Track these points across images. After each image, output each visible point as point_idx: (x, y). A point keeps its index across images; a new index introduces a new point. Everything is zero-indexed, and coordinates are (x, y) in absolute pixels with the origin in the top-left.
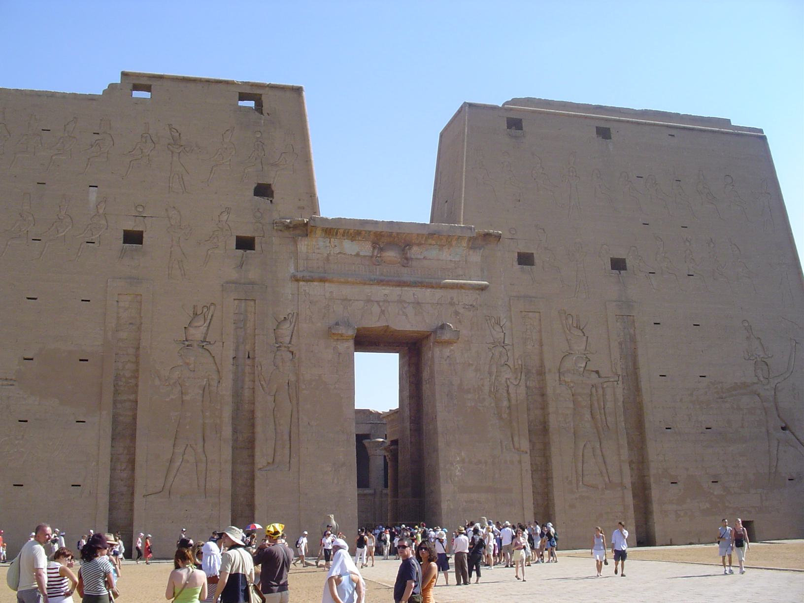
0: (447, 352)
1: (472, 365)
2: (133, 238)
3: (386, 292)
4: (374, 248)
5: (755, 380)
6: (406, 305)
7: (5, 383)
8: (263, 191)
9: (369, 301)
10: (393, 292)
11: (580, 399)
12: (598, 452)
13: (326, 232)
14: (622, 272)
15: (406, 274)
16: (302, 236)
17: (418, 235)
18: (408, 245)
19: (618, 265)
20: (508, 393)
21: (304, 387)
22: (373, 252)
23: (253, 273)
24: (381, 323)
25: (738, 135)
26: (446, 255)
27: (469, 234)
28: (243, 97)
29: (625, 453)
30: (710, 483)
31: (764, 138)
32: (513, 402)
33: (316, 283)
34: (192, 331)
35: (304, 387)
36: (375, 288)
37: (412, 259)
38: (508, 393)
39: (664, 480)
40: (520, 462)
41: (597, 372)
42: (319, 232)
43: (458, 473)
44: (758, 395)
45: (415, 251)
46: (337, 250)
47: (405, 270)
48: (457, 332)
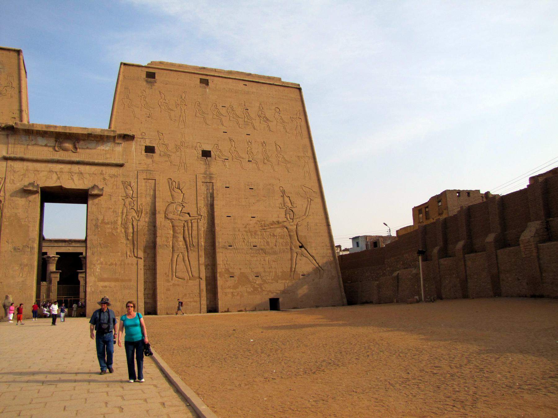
0: (96, 201)
4: (56, 141)
5: (285, 219)
9: (51, 171)
11: (177, 228)
12: (186, 258)
14: (208, 158)
15: (75, 157)
17: (82, 134)
19: (206, 154)
20: (133, 225)
24: (58, 184)
25: (285, 86)
27: (112, 134)
29: (202, 260)
30: (254, 277)
31: (300, 89)
32: (135, 230)
38: (133, 225)
40: (137, 264)
43: (98, 270)
44: (287, 228)
48: (102, 190)
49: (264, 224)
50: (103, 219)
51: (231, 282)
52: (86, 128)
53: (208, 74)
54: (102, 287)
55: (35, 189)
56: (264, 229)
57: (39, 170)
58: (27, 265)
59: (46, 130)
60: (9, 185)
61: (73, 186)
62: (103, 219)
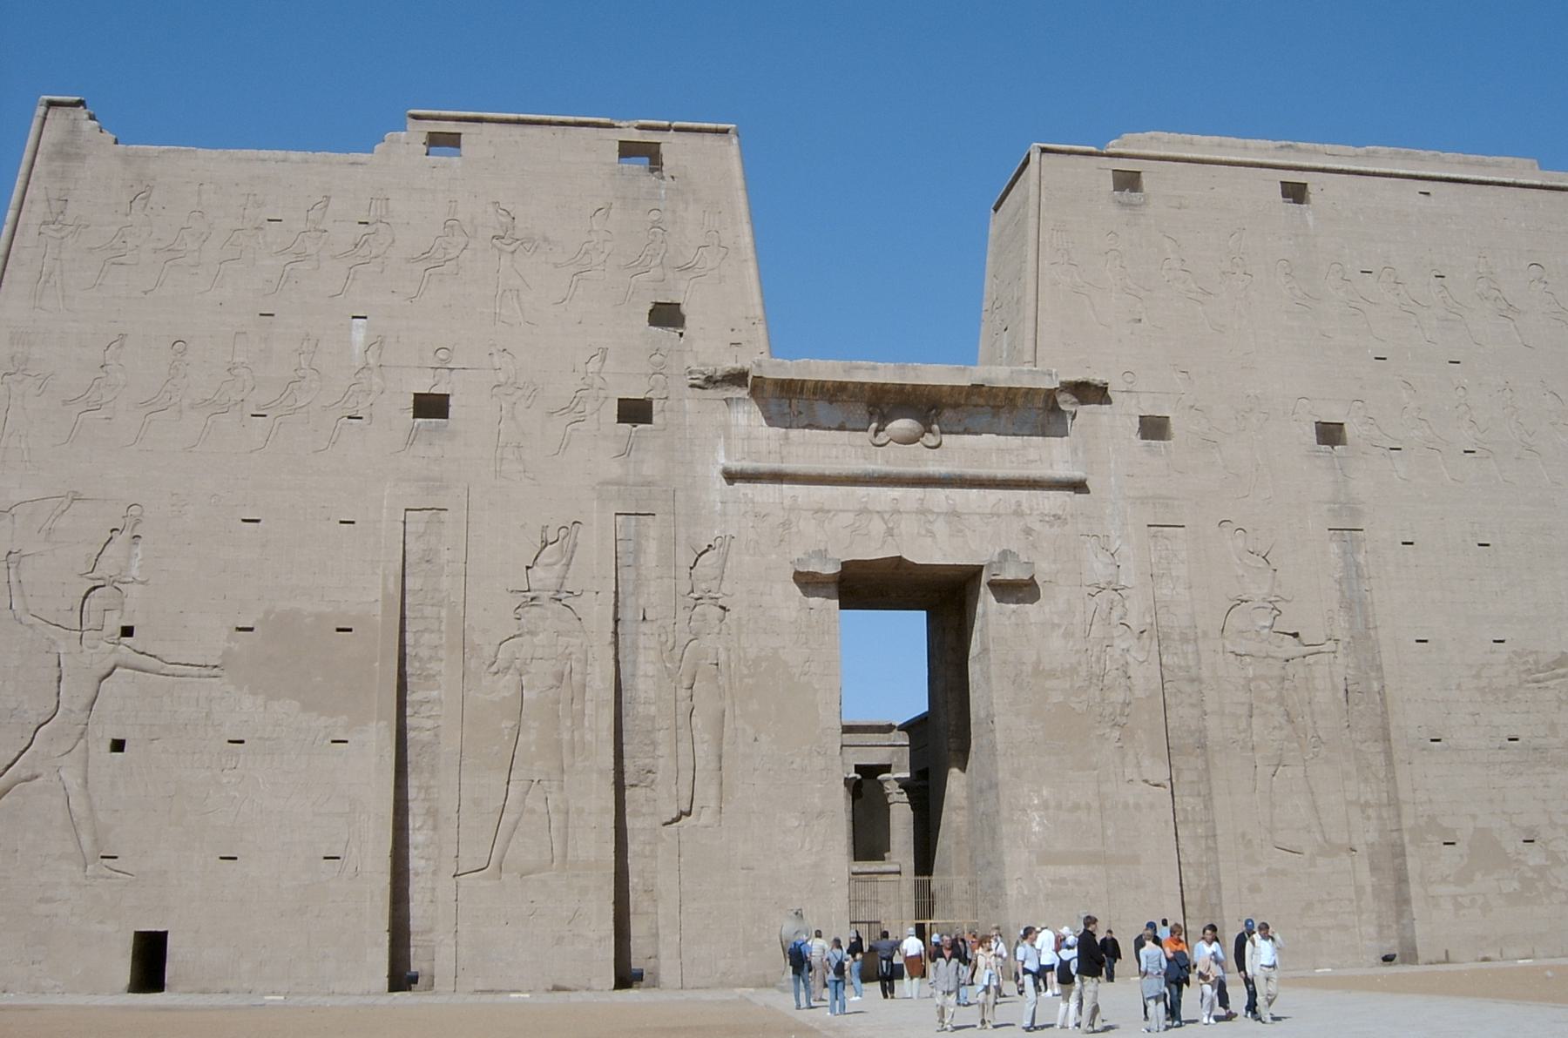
1: (1059, 626)
2: (431, 406)
4: (871, 414)
7: (204, 671)
8: (666, 315)
11: (1264, 686)
17: (953, 387)
19: (1330, 434)
21: (746, 672)
23: (651, 466)
28: (628, 150)
32: (1139, 693)
34: (538, 572)
35: (746, 672)
36: (873, 490)
39: (1429, 837)
41: (1296, 635)
42: (769, 388)
48: (1030, 564)
49: (1536, 662)
50: (1039, 662)
51: (1449, 859)
53: (1307, 164)
54: (1053, 881)
55: (831, 569)
56: (1537, 682)
58: (820, 814)
61: (938, 559)
62: (1039, 662)
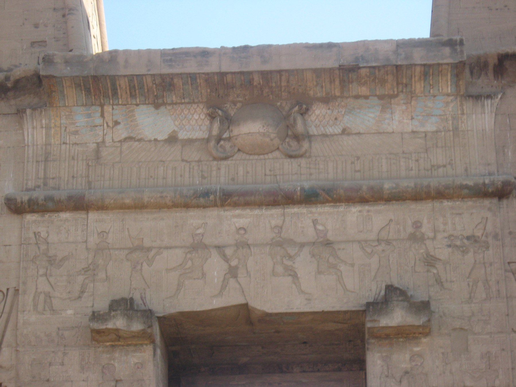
0: (402, 358)
3: (241, 222)
4: (212, 117)
6: (292, 251)
9: (198, 246)
10: (262, 222)
13: (88, 91)
15: (294, 175)
16: (34, 109)
17: (318, 72)
18: (304, 105)
22: (210, 130)
24: (232, 298)
26: (400, 120)
33: (65, 215)
37: (309, 137)
42: (72, 95)
45: (320, 119)
46: (121, 132)
47: (290, 166)
52: (330, 46)
55: (137, 326)
57: (147, 243)
59: (166, 70)
60: (33, 318)
61: (298, 305)
